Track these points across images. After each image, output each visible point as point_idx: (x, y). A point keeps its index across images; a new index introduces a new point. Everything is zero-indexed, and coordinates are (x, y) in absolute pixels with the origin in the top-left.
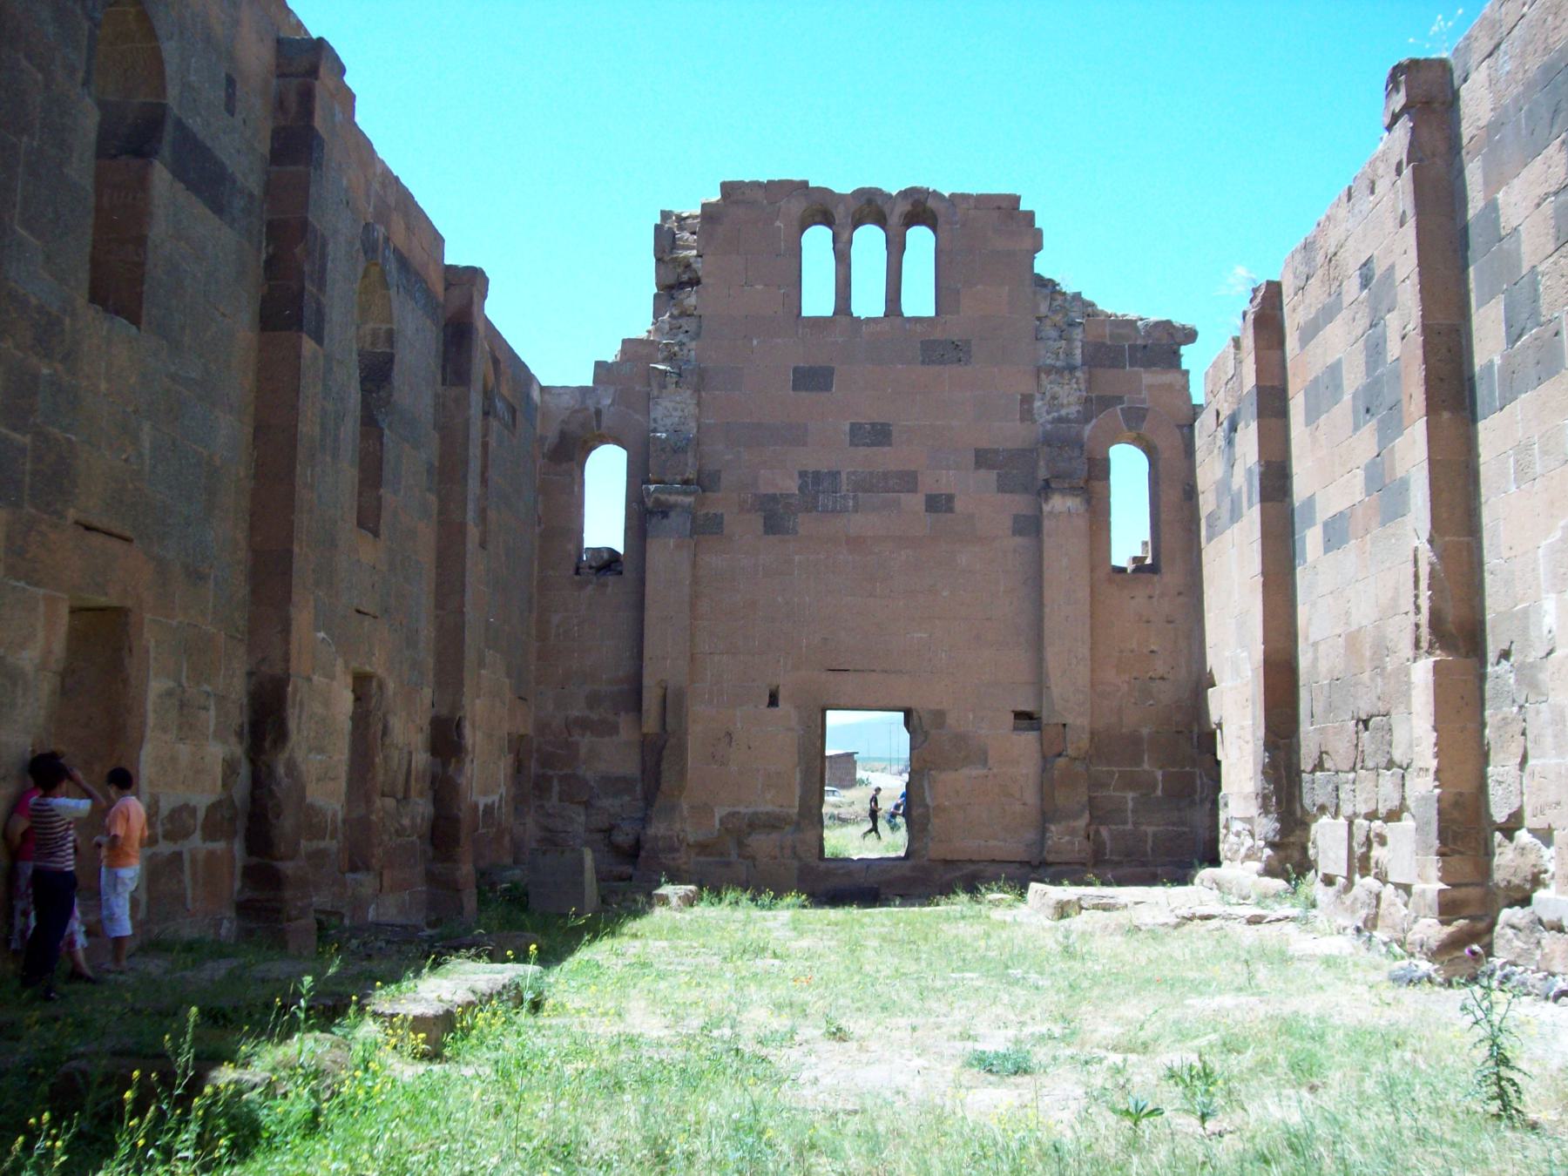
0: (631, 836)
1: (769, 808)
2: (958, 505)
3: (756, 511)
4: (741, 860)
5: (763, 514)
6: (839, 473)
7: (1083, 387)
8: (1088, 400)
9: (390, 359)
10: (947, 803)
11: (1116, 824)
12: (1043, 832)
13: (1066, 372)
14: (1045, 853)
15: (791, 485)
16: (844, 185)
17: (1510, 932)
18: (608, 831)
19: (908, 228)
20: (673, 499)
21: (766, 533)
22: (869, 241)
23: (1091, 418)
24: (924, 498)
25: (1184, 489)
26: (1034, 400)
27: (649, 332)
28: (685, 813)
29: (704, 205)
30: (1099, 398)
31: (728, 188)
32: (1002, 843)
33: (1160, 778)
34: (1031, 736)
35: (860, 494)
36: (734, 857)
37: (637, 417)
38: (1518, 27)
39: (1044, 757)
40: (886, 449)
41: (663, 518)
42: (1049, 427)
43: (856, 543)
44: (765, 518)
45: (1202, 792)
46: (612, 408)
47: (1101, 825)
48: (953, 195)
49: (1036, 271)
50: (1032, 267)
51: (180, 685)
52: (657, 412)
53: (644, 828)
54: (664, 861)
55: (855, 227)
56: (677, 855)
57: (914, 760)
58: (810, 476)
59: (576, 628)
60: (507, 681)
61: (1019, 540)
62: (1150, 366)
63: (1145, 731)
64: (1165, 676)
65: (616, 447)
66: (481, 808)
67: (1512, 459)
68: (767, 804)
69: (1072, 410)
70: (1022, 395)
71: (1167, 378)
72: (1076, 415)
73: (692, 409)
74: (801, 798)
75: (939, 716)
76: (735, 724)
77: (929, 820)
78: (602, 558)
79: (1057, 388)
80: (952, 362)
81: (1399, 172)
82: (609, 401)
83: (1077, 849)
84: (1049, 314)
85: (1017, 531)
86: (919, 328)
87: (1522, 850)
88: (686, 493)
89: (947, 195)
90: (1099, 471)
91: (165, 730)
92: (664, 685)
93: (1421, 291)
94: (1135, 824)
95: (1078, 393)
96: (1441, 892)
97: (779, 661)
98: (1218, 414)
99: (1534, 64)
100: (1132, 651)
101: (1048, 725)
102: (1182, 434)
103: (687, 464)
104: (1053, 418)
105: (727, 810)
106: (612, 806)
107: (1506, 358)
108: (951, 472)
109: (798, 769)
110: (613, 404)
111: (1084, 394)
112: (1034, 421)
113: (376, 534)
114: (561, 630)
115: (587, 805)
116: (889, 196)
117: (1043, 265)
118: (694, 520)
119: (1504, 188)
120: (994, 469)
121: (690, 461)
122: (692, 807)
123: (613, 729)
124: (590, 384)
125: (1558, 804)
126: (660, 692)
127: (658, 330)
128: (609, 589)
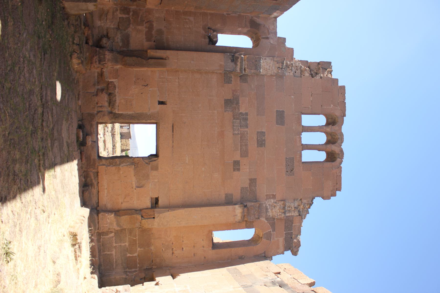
0: (105, 45)
1: (118, 101)
2: (236, 173)
3: (233, 96)
4: (96, 90)
6: (247, 128)
7: (279, 217)
8: (274, 219)
10: (121, 172)
11: (115, 240)
13: (284, 211)
14: (102, 213)
16: (345, 129)
18: (107, 36)
20: (239, 64)
21: (225, 100)
24: (239, 160)
25: (243, 256)
26: (274, 199)
28: (115, 67)
29: (337, 80)
30: (274, 223)
31: (343, 88)
32: (106, 195)
33: (134, 255)
34: (149, 205)
35: (240, 136)
37: (267, 52)
39: (141, 210)
40: (256, 145)
41: (231, 60)
43: (222, 134)
45: (130, 272)
46: (269, 43)
47: (115, 233)
48: (341, 167)
50: (318, 196)
52: (268, 60)
53: (108, 50)
54: (95, 58)
56: (97, 63)
57: (138, 159)
58: (246, 117)
59: (188, 26)
61: (224, 196)
62: (285, 240)
63: (152, 248)
68: (119, 99)
69: (270, 214)
72: (268, 215)
73: (270, 73)
74: (122, 114)
76: (151, 88)
77: (114, 166)
78: (214, 38)
79: (278, 207)
80: (286, 169)
82: (272, 42)
83: (104, 226)
85: (227, 195)
88: (241, 69)
92: (167, 58)
94: (116, 246)
97: (176, 105)
100: (183, 241)
101: (154, 211)
102: (263, 253)
103: (251, 70)
104: (268, 207)
105: (116, 84)
106: (117, 38)
108: (248, 170)
109: (134, 113)
110: (271, 44)
111: (276, 218)
112: (266, 200)
115: (118, 29)
116: (341, 146)
117: (318, 201)
118: (231, 72)
121: (253, 71)
122: (117, 70)
123: (148, 39)
124: (278, 36)
126: (164, 57)
127: (296, 61)
128: (203, 40)
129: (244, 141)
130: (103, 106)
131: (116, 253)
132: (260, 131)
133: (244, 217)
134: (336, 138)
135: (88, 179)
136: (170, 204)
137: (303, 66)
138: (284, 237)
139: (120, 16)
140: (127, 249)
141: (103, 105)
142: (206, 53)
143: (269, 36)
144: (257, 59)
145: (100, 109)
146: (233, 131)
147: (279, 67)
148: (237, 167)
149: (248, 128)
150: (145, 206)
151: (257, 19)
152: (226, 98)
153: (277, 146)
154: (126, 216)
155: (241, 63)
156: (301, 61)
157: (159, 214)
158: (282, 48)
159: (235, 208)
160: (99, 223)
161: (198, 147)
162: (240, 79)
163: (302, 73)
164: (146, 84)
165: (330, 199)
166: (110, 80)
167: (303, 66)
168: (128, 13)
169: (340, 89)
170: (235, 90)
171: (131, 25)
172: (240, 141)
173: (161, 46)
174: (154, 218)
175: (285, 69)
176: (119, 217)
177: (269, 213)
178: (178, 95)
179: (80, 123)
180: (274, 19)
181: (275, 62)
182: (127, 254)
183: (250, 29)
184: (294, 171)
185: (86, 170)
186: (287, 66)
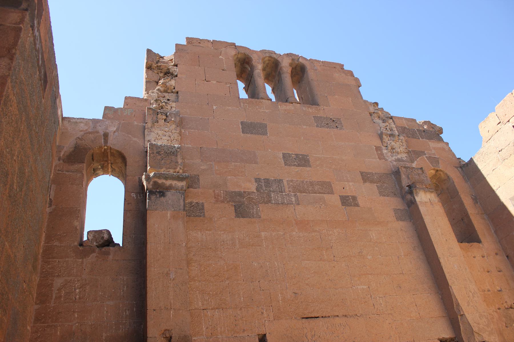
15: (252, 187)
20: (168, 183)
21: (237, 216)
24: (339, 198)
35: (298, 194)
37: (135, 139)
40: (308, 169)
41: (160, 196)
42: (395, 163)
46: (116, 134)
59: (78, 291)
61: (401, 223)
78: (103, 237)
82: (115, 129)
84: (375, 111)
100: (489, 291)
102: (458, 169)
103: (177, 162)
108: (351, 184)
110: (117, 130)
114: (63, 293)
120: (374, 183)
124: (101, 118)
128: (111, 257)
129: (306, 186)
132: (283, 160)
134: (267, 62)
136: (446, 316)
143: (102, 133)
144: (155, 152)
146: (293, 204)
147: (165, 120)
148: (351, 200)
149: (283, 179)
151: (65, 149)
152: (234, 214)
153: (302, 138)
157: (474, 333)
161: (334, 267)
162: (192, 188)
169: (192, 43)
170: (215, 198)
172: (306, 193)
177: (403, 157)
178: (241, 309)
180: (66, 122)
181: (155, 127)
184: (334, 118)
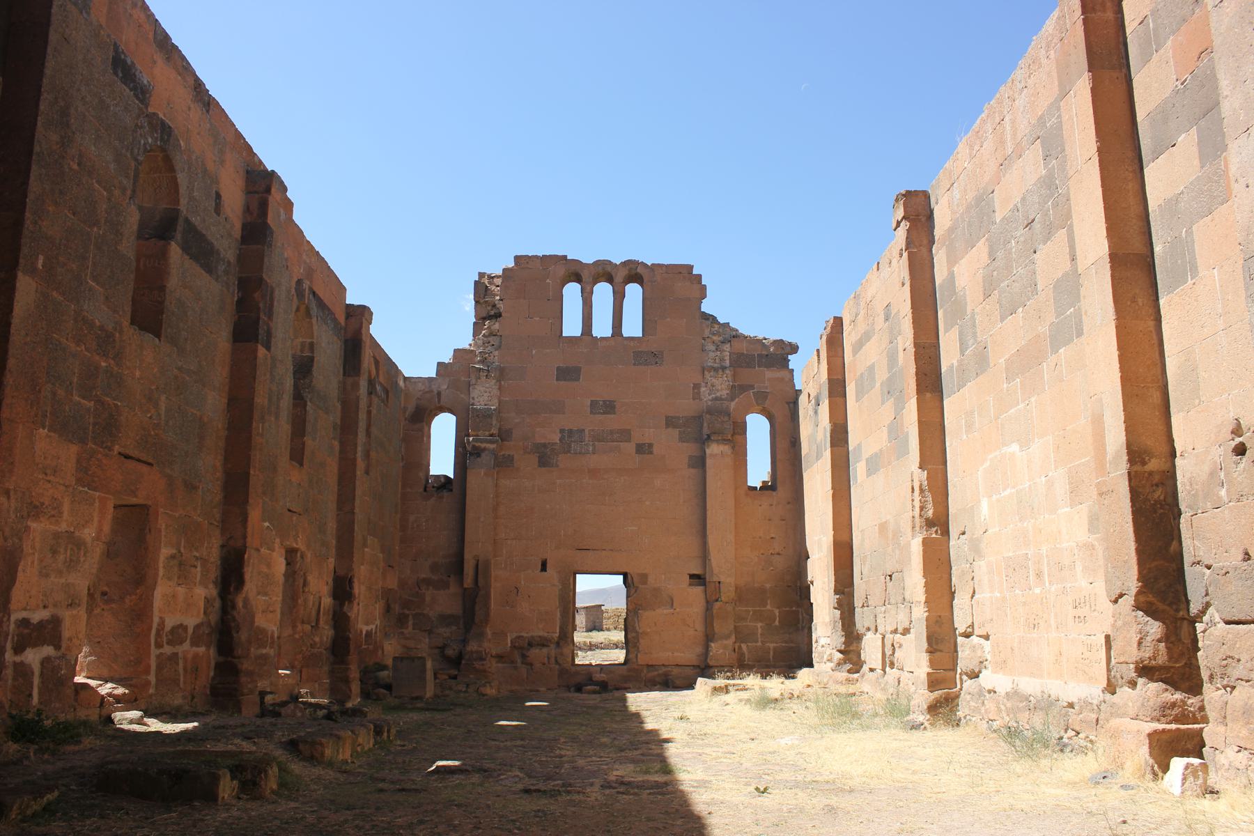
0: (456, 651)
1: (541, 633)
2: (655, 450)
4: (524, 666)
5: (538, 455)
6: (584, 430)
9: (312, 359)
12: (707, 648)
13: (720, 371)
14: (708, 661)
16: (588, 259)
17: (968, 697)
18: (442, 648)
19: (626, 285)
20: (483, 445)
21: (540, 466)
22: (603, 292)
23: (735, 399)
24: (635, 445)
27: (470, 345)
28: (490, 637)
31: (517, 258)
32: (682, 654)
33: (777, 614)
34: (700, 588)
36: (519, 664)
37: (462, 396)
38: (962, 175)
39: (707, 602)
40: (613, 416)
41: (478, 457)
43: (594, 473)
44: (539, 457)
45: (803, 622)
46: (447, 391)
47: (742, 642)
49: (702, 310)
51: (180, 552)
53: (464, 646)
54: (477, 666)
55: (595, 283)
56: (485, 662)
57: (629, 604)
60: (381, 555)
61: (693, 471)
63: (768, 586)
64: (781, 552)
65: (450, 414)
66: (364, 633)
67: (963, 421)
68: (538, 632)
69: (724, 393)
70: (694, 384)
71: (781, 374)
72: (726, 396)
73: (496, 392)
74: (560, 627)
75: (644, 578)
76: (520, 583)
79: (714, 380)
80: (652, 365)
81: (901, 255)
82: (446, 387)
84: (710, 336)
86: (632, 344)
87: (973, 648)
89: (649, 264)
90: (741, 429)
91: (169, 579)
93: (913, 323)
94: (762, 642)
95: (727, 383)
96: (928, 674)
97: (547, 544)
98: (809, 395)
99: (970, 196)
100: (760, 538)
101: (709, 582)
102: (789, 406)
103: (492, 425)
105: (515, 635)
107: (960, 362)
109: (558, 609)
110: (448, 388)
112: (701, 400)
113: (301, 464)
114: (415, 526)
115: (430, 632)
117: (706, 307)
118: (496, 458)
119: (957, 265)
121: (494, 422)
122: (494, 633)
123: (446, 586)
124: (435, 376)
125: (992, 620)
127: (476, 344)
128: (444, 500)
130: (548, 654)
131: (772, 642)
133: (724, 440)
135: (657, 679)
137: (484, 332)
138: (766, 369)
139: (410, 628)
140: (767, 624)
141: (546, 656)
142: (467, 497)
143: (436, 392)
145: (553, 660)
150: (702, 596)
154: (715, 625)
155: (482, 441)
156: (474, 335)
158: (454, 369)
159: (711, 455)
160: (722, 664)
163: (494, 334)
164: (516, 590)
165: (705, 286)
166: (509, 645)
167: (484, 332)
168: (407, 616)
171: (425, 612)
173: (457, 565)
174: (719, 582)
175: (489, 364)
176: (716, 636)
179: (572, 689)
180: (407, 383)
182: (776, 626)
183: (424, 424)
185: (643, 683)
186: (483, 361)
